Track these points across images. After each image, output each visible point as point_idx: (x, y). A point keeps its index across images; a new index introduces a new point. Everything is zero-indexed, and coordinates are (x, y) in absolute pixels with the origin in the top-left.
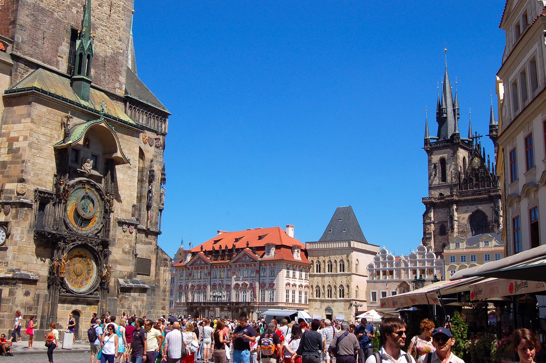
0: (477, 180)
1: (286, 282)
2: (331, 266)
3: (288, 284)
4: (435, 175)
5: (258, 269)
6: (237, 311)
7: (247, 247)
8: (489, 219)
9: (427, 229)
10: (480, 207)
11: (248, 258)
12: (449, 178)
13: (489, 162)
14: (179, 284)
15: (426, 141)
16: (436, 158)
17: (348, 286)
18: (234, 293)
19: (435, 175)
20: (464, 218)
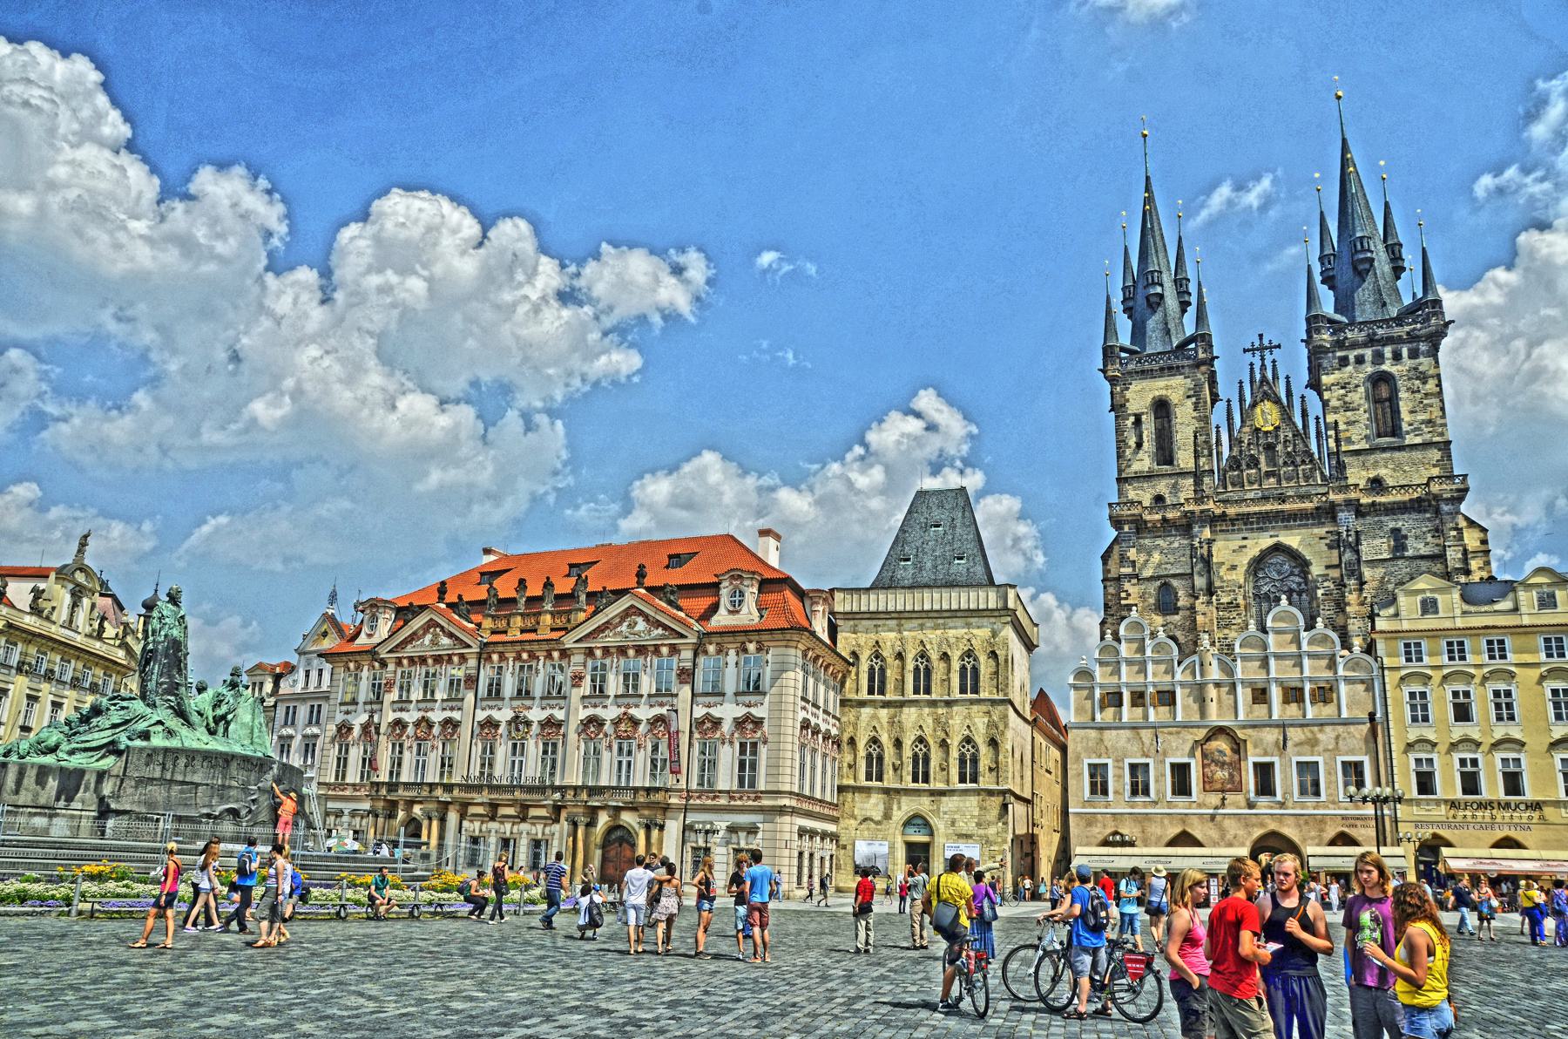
0: (1272, 461)
1: (802, 715)
2: (928, 671)
3: (806, 725)
4: (1139, 445)
5: (689, 665)
6: (591, 824)
7: (640, 584)
8: (1316, 570)
9: (1123, 595)
10: (1292, 539)
11: (641, 625)
12: (1185, 459)
13: (1304, 414)
14: (340, 718)
15: (1108, 353)
16: (1140, 396)
17: (993, 743)
18: (574, 748)
19: (1139, 445)
20: (1234, 567)
